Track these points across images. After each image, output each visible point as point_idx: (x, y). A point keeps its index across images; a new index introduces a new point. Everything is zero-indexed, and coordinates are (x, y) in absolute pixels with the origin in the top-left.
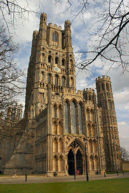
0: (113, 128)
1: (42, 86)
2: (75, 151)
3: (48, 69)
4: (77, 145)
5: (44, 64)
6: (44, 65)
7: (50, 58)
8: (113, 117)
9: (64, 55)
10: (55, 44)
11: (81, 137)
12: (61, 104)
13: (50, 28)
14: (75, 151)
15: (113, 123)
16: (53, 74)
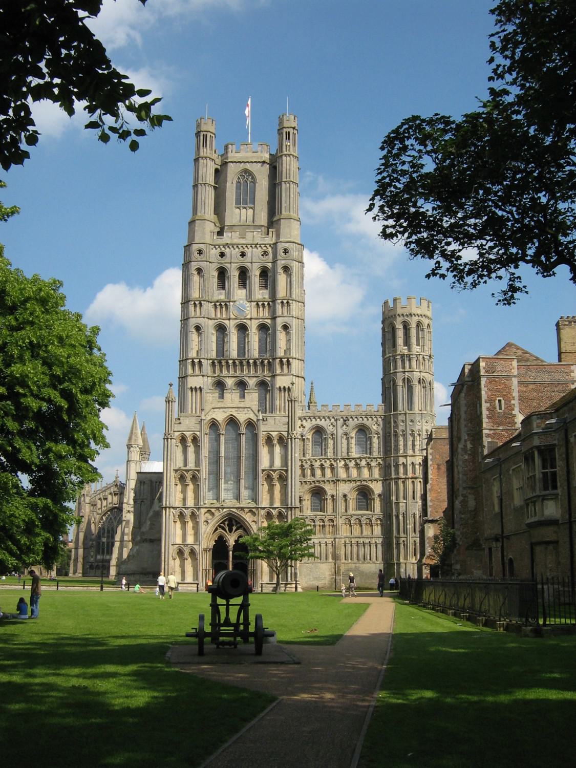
0: (410, 468)
1: (197, 367)
2: (231, 540)
3: (216, 315)
4: (234, 528)
5: (200, 303)
6: (200, 303)
7: (222, 273)
8: (413, 435)
9: (265, 253)
10: (243, 218)
11: (242, 509)
12: (198, 433)
13: (226, 163)
14: (231, 540)
15: (410, 452)
16: (231, 325)
